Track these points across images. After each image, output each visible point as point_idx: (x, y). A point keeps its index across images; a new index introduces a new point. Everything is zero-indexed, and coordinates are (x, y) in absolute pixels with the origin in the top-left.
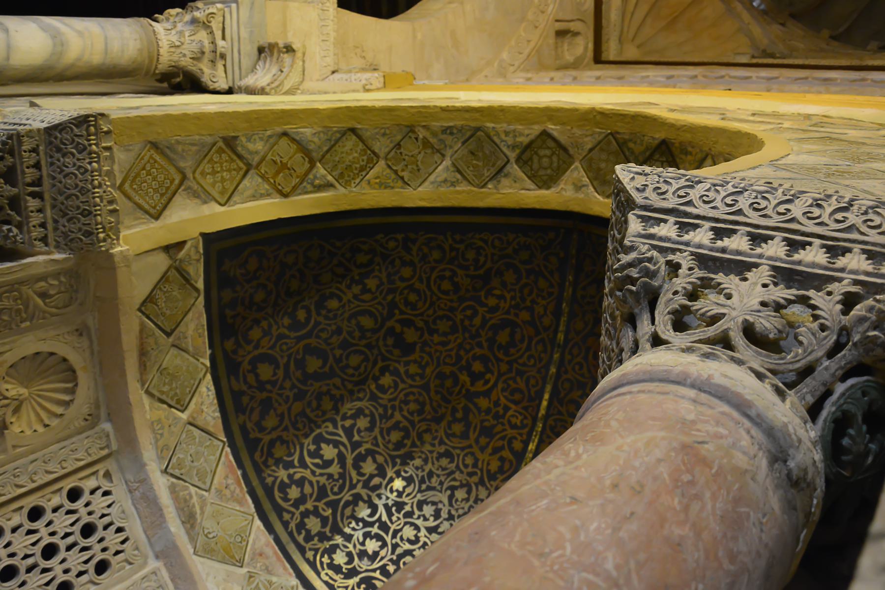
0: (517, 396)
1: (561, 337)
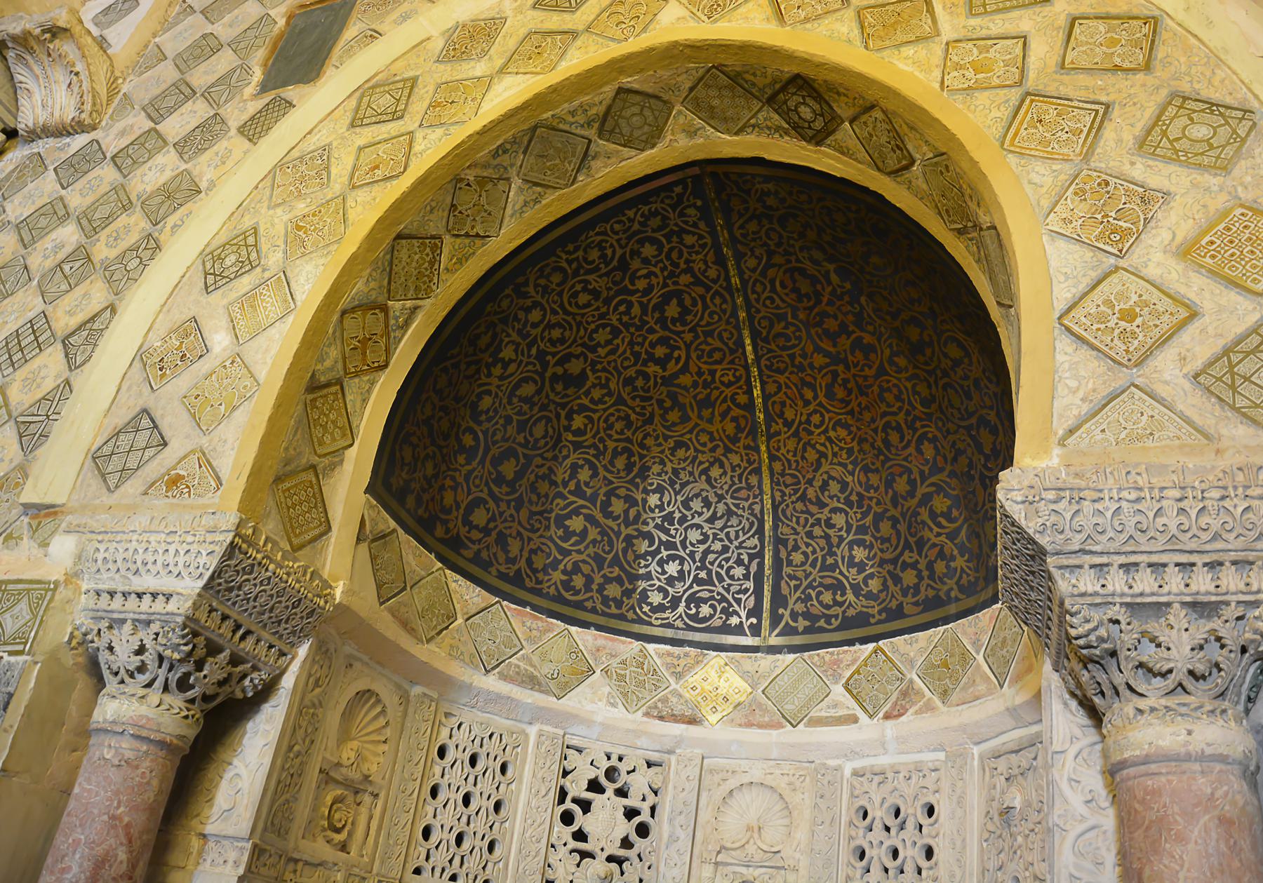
0: (717, 356)
1: (735, 281)
